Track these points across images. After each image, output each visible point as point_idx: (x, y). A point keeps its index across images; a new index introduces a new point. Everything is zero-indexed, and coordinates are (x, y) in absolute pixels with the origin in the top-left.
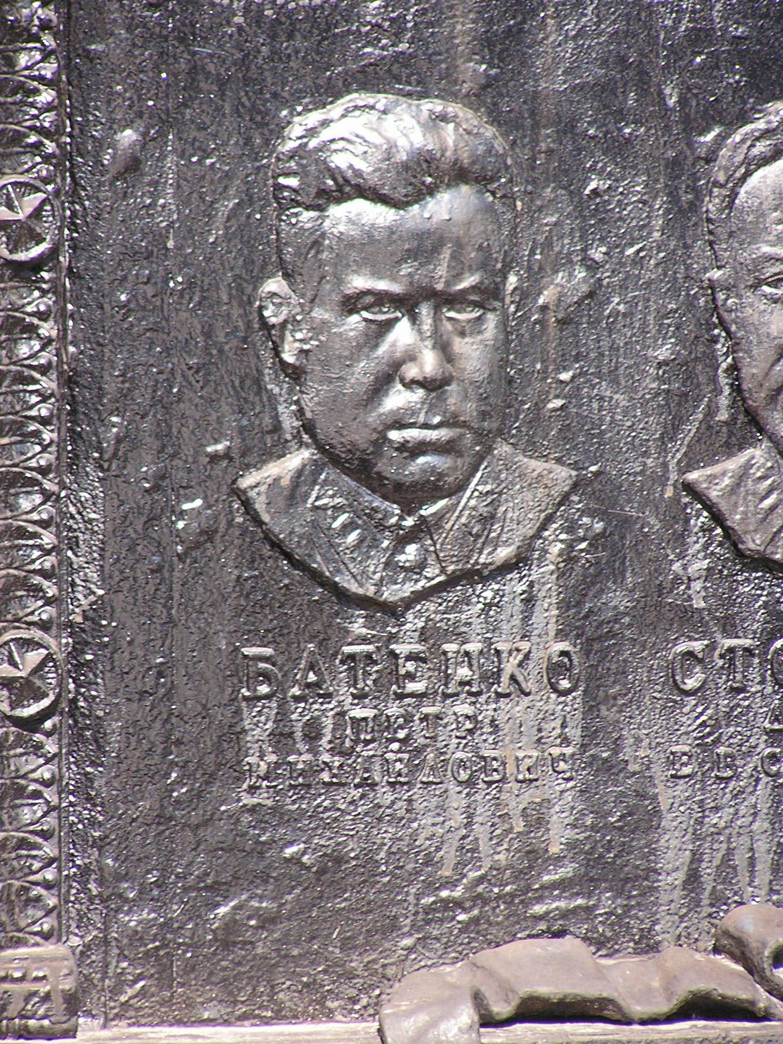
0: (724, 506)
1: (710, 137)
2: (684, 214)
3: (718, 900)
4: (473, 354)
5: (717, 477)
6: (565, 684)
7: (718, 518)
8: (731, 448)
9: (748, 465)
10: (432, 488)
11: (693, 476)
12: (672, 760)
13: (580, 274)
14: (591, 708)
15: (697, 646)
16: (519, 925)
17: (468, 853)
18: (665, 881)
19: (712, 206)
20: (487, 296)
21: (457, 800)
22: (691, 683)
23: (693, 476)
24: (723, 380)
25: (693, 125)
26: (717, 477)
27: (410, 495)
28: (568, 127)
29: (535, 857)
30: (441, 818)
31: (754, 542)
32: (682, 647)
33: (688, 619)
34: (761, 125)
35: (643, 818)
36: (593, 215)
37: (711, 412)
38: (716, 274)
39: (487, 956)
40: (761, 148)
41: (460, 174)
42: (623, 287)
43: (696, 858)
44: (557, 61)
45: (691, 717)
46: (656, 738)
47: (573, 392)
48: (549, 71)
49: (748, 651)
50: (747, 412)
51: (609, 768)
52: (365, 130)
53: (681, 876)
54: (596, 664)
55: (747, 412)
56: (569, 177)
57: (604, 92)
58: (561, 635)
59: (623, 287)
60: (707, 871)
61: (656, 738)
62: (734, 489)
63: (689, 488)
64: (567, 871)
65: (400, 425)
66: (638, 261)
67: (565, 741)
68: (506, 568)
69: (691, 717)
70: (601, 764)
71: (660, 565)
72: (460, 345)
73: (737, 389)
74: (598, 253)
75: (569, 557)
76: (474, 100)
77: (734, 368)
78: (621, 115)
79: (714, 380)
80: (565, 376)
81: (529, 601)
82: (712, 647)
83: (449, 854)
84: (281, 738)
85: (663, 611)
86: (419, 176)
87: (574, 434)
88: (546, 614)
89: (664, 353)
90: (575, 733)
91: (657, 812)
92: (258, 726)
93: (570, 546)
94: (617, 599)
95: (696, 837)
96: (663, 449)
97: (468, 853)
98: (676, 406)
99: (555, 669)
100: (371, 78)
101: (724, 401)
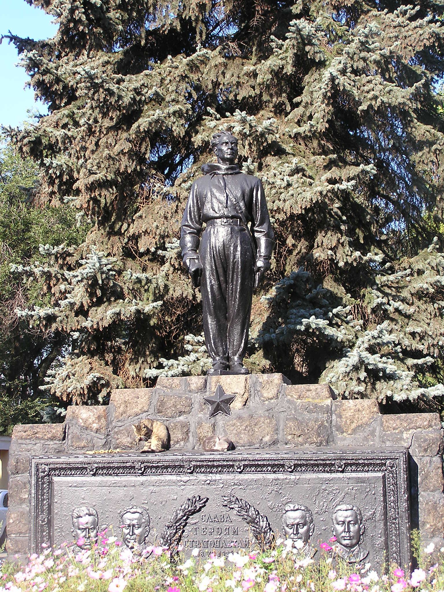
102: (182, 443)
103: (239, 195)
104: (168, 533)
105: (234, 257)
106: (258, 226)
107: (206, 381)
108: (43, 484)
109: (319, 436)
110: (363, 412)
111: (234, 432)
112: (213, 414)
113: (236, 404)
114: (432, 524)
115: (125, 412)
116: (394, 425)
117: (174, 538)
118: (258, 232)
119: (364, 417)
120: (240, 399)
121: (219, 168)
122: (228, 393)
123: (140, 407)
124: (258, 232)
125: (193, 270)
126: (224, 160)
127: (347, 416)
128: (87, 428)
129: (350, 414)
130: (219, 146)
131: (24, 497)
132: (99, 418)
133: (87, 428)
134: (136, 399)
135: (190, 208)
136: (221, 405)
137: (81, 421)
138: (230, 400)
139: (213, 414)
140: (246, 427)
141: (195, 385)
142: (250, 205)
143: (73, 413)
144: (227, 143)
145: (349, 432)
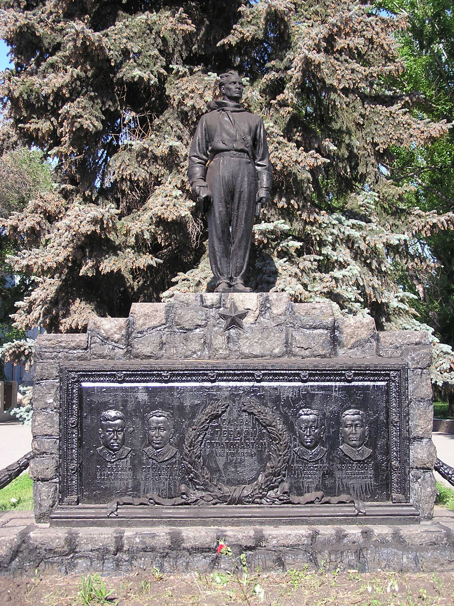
2: (143, 423)
3: (147, 493)
4: (120, 436)
5: (146, 450)
10: (116, 450)
16: (125, 494)
17: (120, 487)
20: (122, 431)
21: (119, 482)
26: (146, 450)
27: (114, 451)
29: (128, 488)
30: (117, 484)
33: (144, 464)
36: (134, 423)
39: (122, 498)
41: (119, 418)
46: (141, 476)
52: (112, 413)
54: (134, 468)
61: (141, 476)
65: (112, 443)
68: (124, 458)
69: (144, 474)
70: (135, 479)
71: (141, 458)
72: (119, 436)
75: (131, 457)
76: (120, 411)
81: (127, 462)
83: (118, 487)
84: (101, 475)
85: (141, 463)
86: (115, 418)
87: (131, 445)
88: (129, 463)
92: (98, 474)
94: (136, 462)
97: (120, 487)
98: (142, 442)
99: (129, 469)
100: (111, 408)
102: (199, 353)
103: (247, 130)
104: (193, 435)
105: (241, 186)
106: (260, 160)
107: (221, 297)
108: (73, 389)
109: (324, 350)
110: (362, 329)
111: (247, 344)
112: (227, 328)
113: (249, 319)
114: (423, 427)
115: (144, 324)
116: (390, 341)
117: (198, 440)
118: (259, 165)
119: (363, 333)
120: (252, 315)
121: (226, 105)
122: (241, 309)
123: (158, 320)
124: (259, 165)
125: (203, 196)
126: (231, 98)
127: (348, 332)
128: (109, 338)
129: (350, 330)
130: (226, 85)
131: (49, 402)
132: (121, 328)
133: (107, 339)
134: (155, 313)
135: (199, 140)
136: (235, 321)
137: (103, 332)
138: (243, 316)
139: (227, 328)
140: (259, 340)
141: (210, 301)
142: (255, 140)
143: (95, 324)
144: (235, 83)
145: (349, 347)
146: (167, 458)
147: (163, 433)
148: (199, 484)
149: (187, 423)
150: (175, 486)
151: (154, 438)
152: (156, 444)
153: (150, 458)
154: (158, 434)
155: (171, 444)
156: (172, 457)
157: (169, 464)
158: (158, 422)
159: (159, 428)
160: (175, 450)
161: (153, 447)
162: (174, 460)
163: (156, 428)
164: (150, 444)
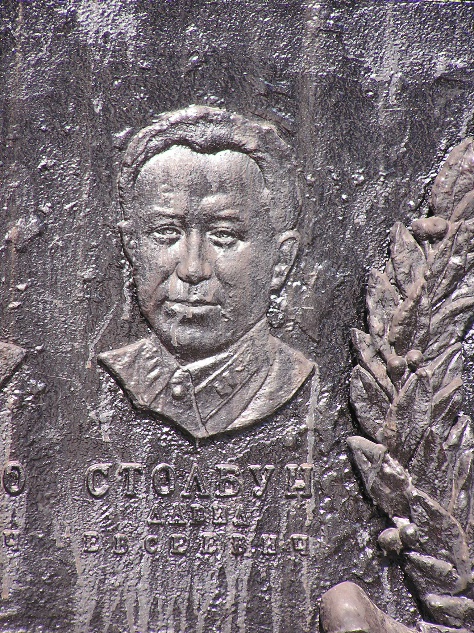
0: (123, 376)
1: (122, 134)
2: (104, 184)
6: (15, 488)
7: (120, 383)
8: (131, 336)
9: (141, 350)
11: (104, 355)
12: (85, 540)
13: (33, 220)
14: (32, 504)
15: (104, 467)
18: (78, 619)
19: (122, 179)
22: (99, 491)
23: (104, 355)
24: (127, 293)
25: (110, 127)
26: (120, 357)
28: (27, 125)
31: (143, 400)
32: (94, 467)
33: (100, 449)
34: (157, 127)
35: (66, 578)
37: (117, 315)
38: (123, 224)
40: (156, 142)
42: (62, 229)
43: (99, 605)
44: (22, 80)
45: (98, 513)
47: (26, 298)
48: (17, 87)
49: (138, 472)
50: (142, 314)
51: (44, 545)
53: (89, 616)
55: (142, 314)
56: (28, 158)
57: (52, 99)
58: (13, 456)
59: (62, 229)
60: (107, 614)
61: (75, 526)
62: (131, 364)
63: (101, 363)
64: (13, 610)
66: (72, 213)
67: (14, 525)
73: (135, 299)
74: (45, 208)
77: (134, 286)
78: (63, 117)
79: (121, 293)
80: (21, 287)
82: (113, 468)
89: (87, 274)
90: (21, 521)
91: (74, 575)
93: (21, 398)
95: (100, 592)
96: (85, 338)
101: (127, 307)
146: (249, 416)
147: (230, 257)
148: (445, 584)
149: (381, 190)
150: (292, 589)
151: (176, 286)
152: (186, 321)
153: (147, 413)
154: (202, 257)
155: (275, 328)
156: (281, 410)
157: (259, 454)
158: (200, 187)
159: (207, 222)
160: (303, 365)
161: (165, 341)
162: (289, 431)
163: (183, 223)
164: (143, 321)
